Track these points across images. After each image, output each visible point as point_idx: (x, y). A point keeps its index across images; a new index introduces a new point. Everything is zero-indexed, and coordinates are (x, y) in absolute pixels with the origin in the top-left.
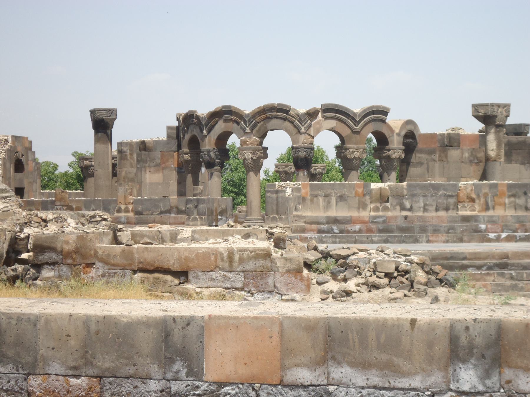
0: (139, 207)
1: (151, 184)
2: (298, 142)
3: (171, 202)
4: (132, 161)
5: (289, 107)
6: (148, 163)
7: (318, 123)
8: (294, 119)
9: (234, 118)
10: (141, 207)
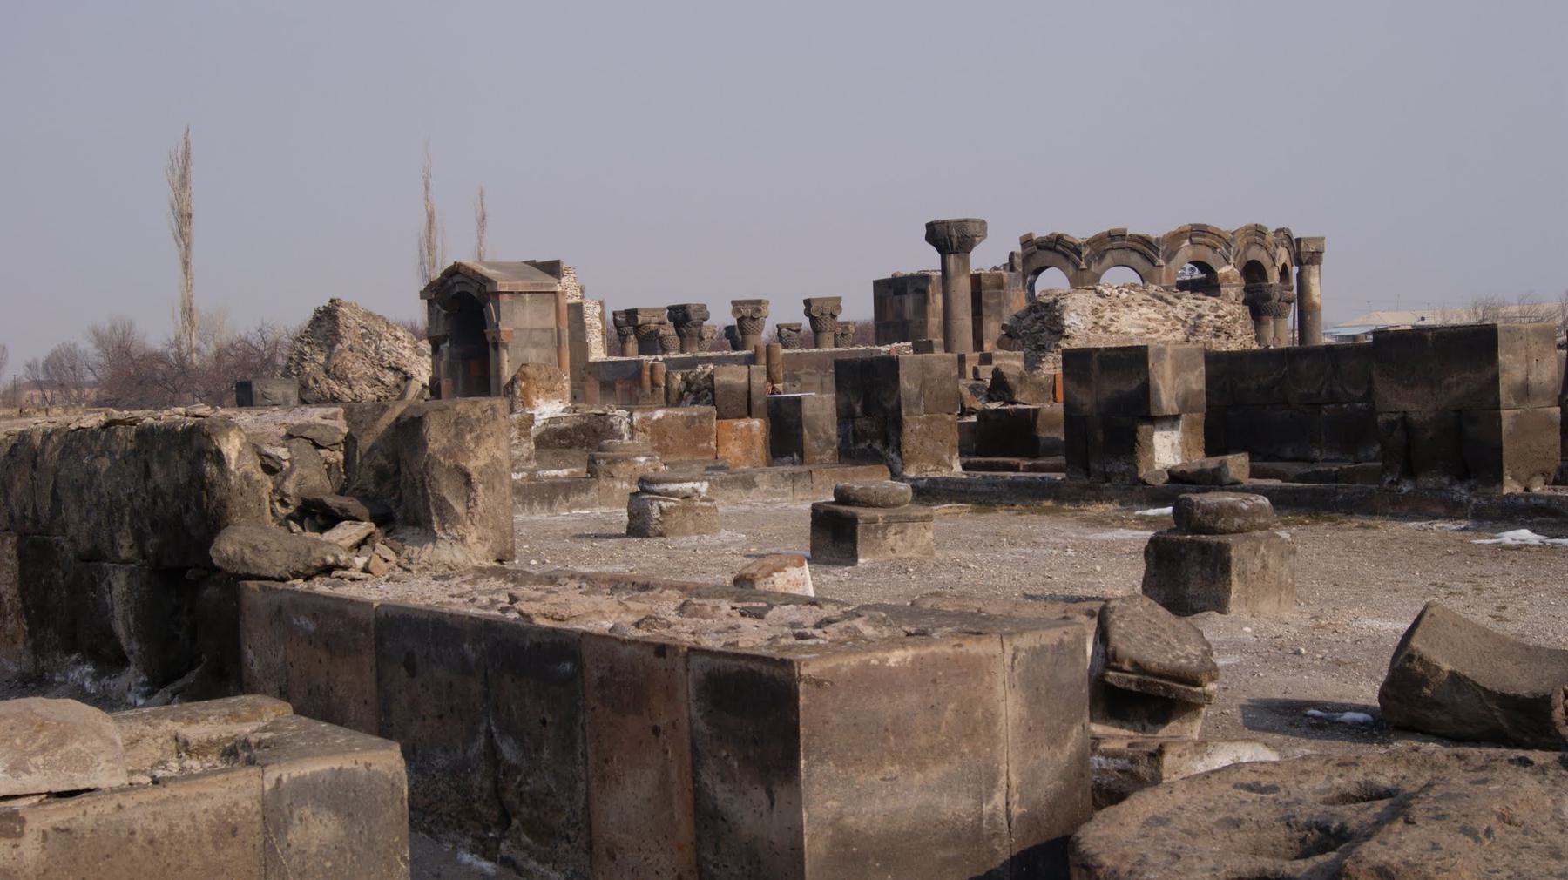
5: (1266, 229)
9: (1208, 240)
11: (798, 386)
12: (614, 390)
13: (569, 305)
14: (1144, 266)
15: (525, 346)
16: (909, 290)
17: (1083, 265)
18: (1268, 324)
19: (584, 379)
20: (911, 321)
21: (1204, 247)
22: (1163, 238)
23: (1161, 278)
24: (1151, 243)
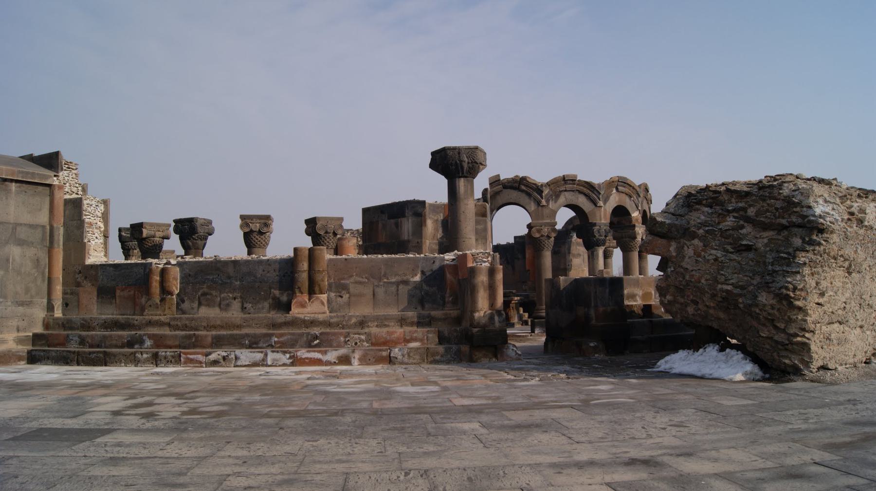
11: (346, 296)
12: (114, 297)
13: (65, 200)
15: (7, 243)
16: (408, 213)
17: (544, 202)
19: (78, 285)
20: (409, 241)
21: (624, 195)
23: (600, 216)
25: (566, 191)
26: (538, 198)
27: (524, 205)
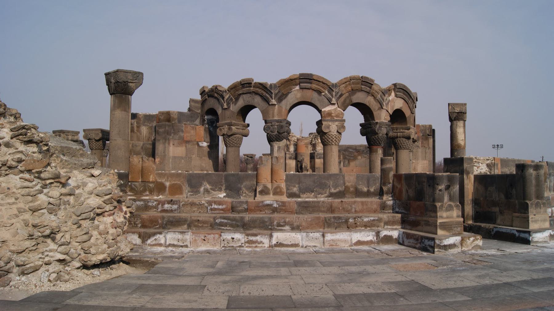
0: (295, 186)
1: (174, 157)
2: (380, 118)
3: (346, 178)
4: (139, 134)
5: (373, 81)
6: (172, 135)
7: (393, 100)
8: (377, 94)
10: (297, 186)
14: (264, 104)
17: (225, 106)
18: (376, 151)
21: (311, 91)
22: (275, 85)
23: (273, 114)
24: (266, 88)
25: (243, 94)
26: (222, 102)
27: (319, 106)
